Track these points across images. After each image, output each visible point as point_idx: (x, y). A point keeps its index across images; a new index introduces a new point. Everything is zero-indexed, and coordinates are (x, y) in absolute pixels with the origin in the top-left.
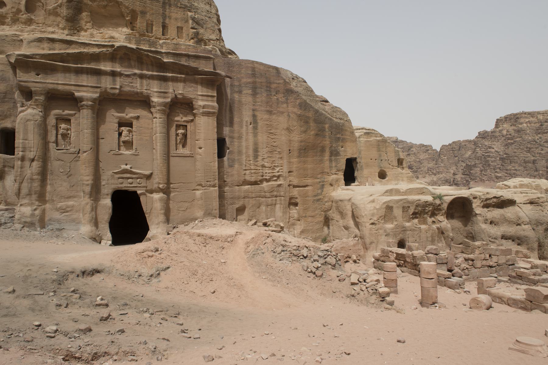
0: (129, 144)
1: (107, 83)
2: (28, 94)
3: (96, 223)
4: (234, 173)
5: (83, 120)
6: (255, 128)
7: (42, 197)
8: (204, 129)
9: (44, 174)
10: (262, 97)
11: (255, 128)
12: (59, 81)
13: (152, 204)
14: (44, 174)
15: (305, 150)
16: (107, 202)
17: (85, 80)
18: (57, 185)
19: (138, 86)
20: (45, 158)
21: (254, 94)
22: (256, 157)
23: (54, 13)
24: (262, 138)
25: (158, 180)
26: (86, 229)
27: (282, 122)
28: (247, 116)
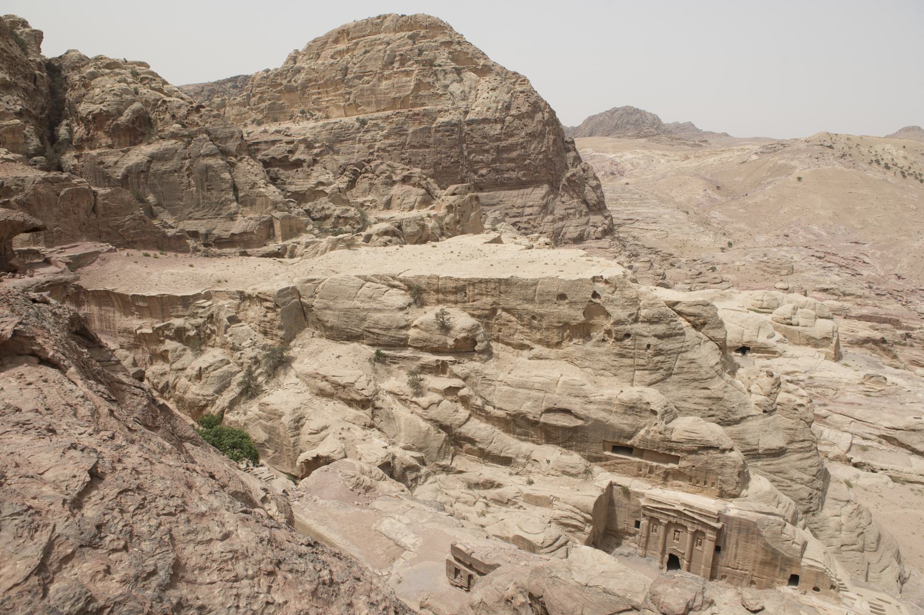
0: (678, 539)
1: (671, 519)
2: (644, 515)
3: (662, 563)
4: (722, 561)
5: (661, 530)
6: (737, 547)
7: (646, 548)
8: (708, 547)
9: (647, 541)
10: (743, 534)
11: (737, 547)
12: (655, 515)
13: (684, 563)
14: (647, 541)
15: (764, 563)
16: (667, 556)
17: (663, 516)
18: (651, 545)
19: (683, 522)
20: (648, 537)
21: (739, 532)
22: (735, 558)
23: (658, 475)
24: (740, 551)
25: (686, 556)
26: (658, 564)
27: (754, 547)
28: (733, 540)
